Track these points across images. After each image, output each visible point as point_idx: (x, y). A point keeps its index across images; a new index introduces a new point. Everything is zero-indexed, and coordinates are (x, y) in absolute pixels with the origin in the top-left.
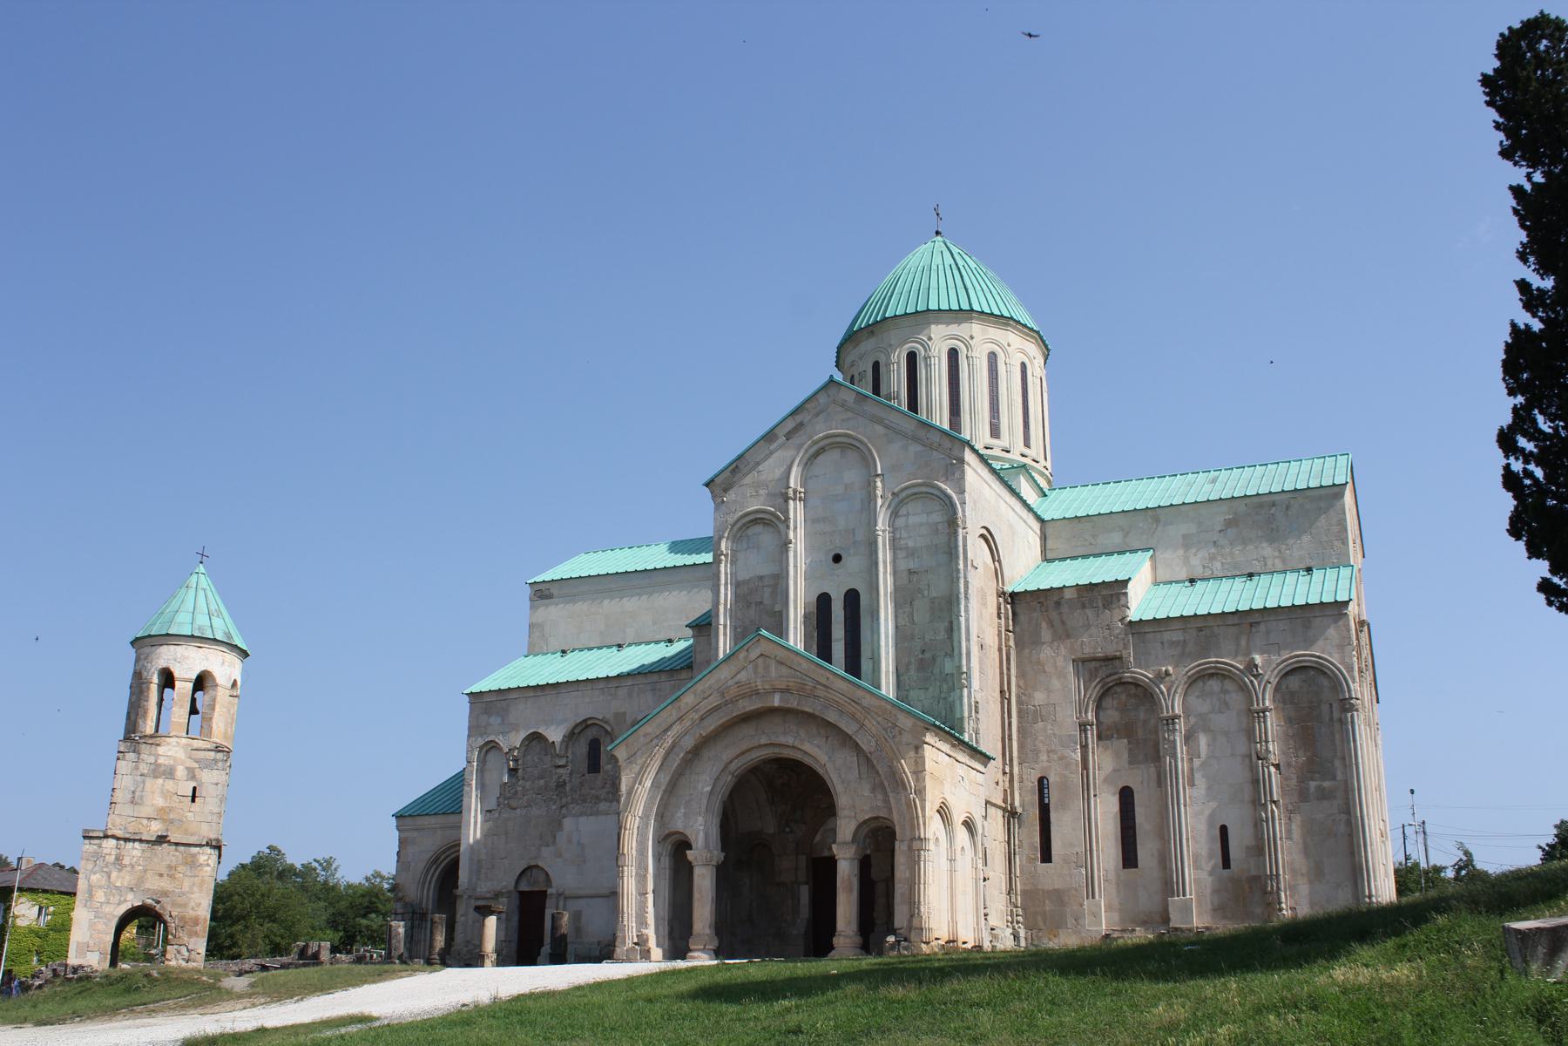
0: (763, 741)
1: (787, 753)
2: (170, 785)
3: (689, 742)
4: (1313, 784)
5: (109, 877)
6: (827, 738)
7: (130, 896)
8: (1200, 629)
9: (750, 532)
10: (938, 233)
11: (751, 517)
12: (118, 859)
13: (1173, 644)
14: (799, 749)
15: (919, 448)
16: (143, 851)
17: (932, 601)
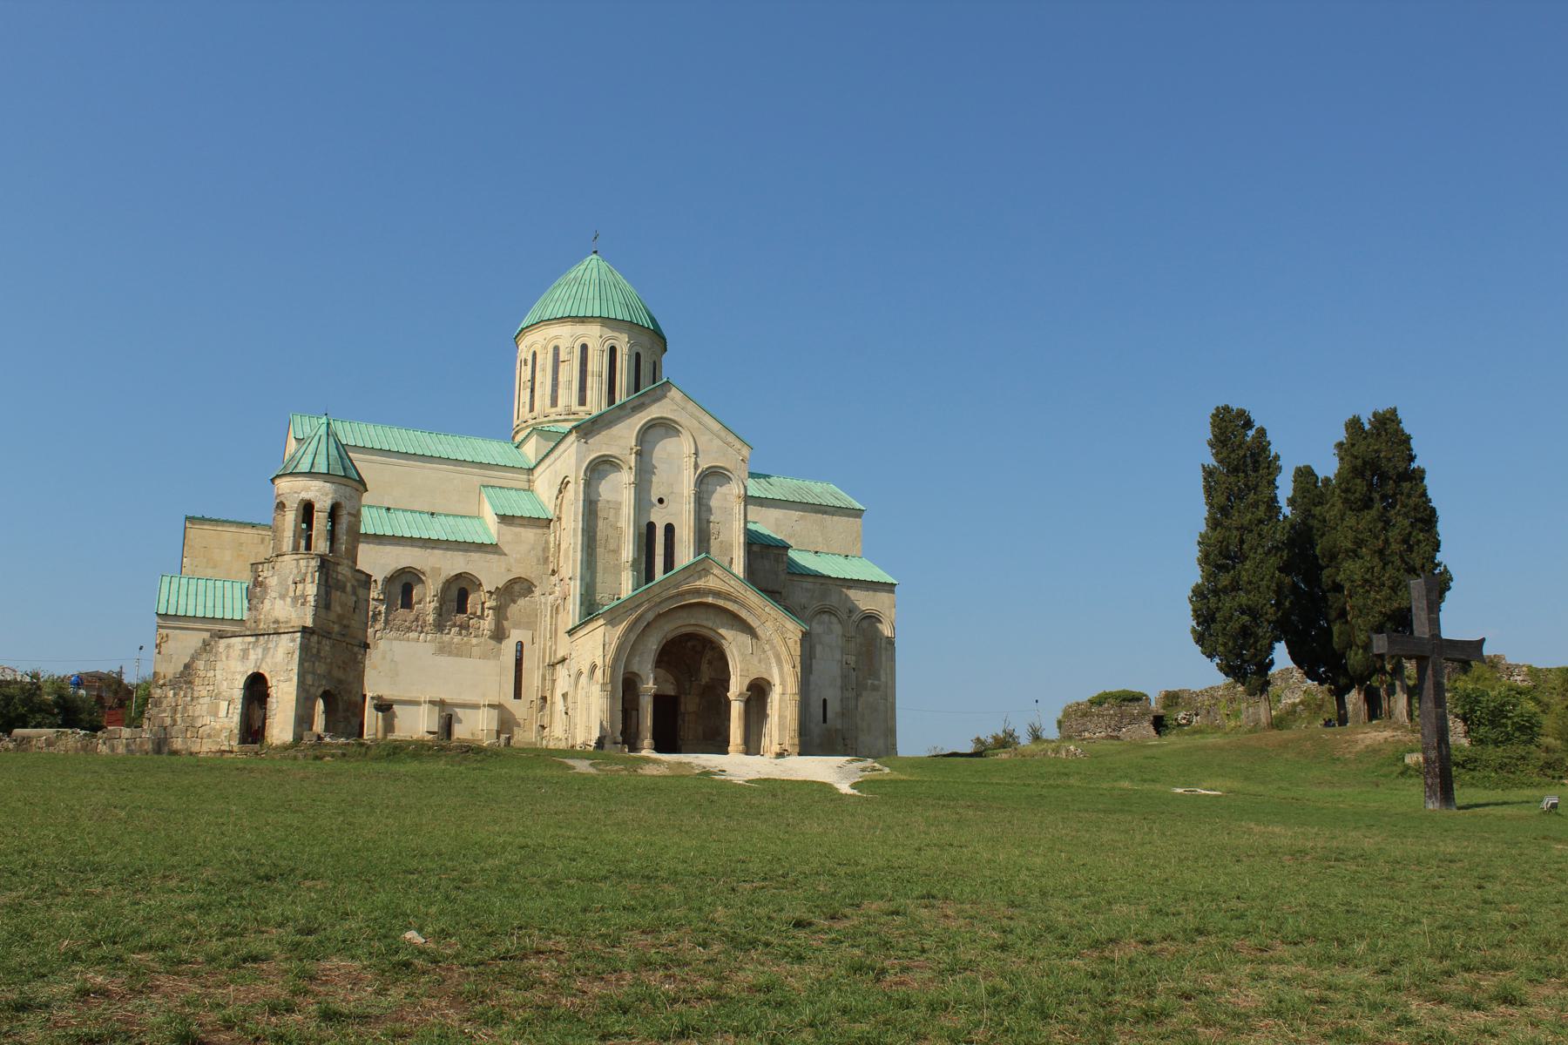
0: (693, 622)
1: (704, 632)
2: (343, 594)
3: (650, 616)
4: (870, 682)
5: (314, 663)
6: (733, 626)
7: (324, 682)
8: (822, 584)
9: (601, 467)
10: (595, 252)
11: (605, 459)
12: (318, 651)
13: (807, 590)
14: (714, 631)
15: (721, 443)
16: (331, 648)
17: (721, 542)
